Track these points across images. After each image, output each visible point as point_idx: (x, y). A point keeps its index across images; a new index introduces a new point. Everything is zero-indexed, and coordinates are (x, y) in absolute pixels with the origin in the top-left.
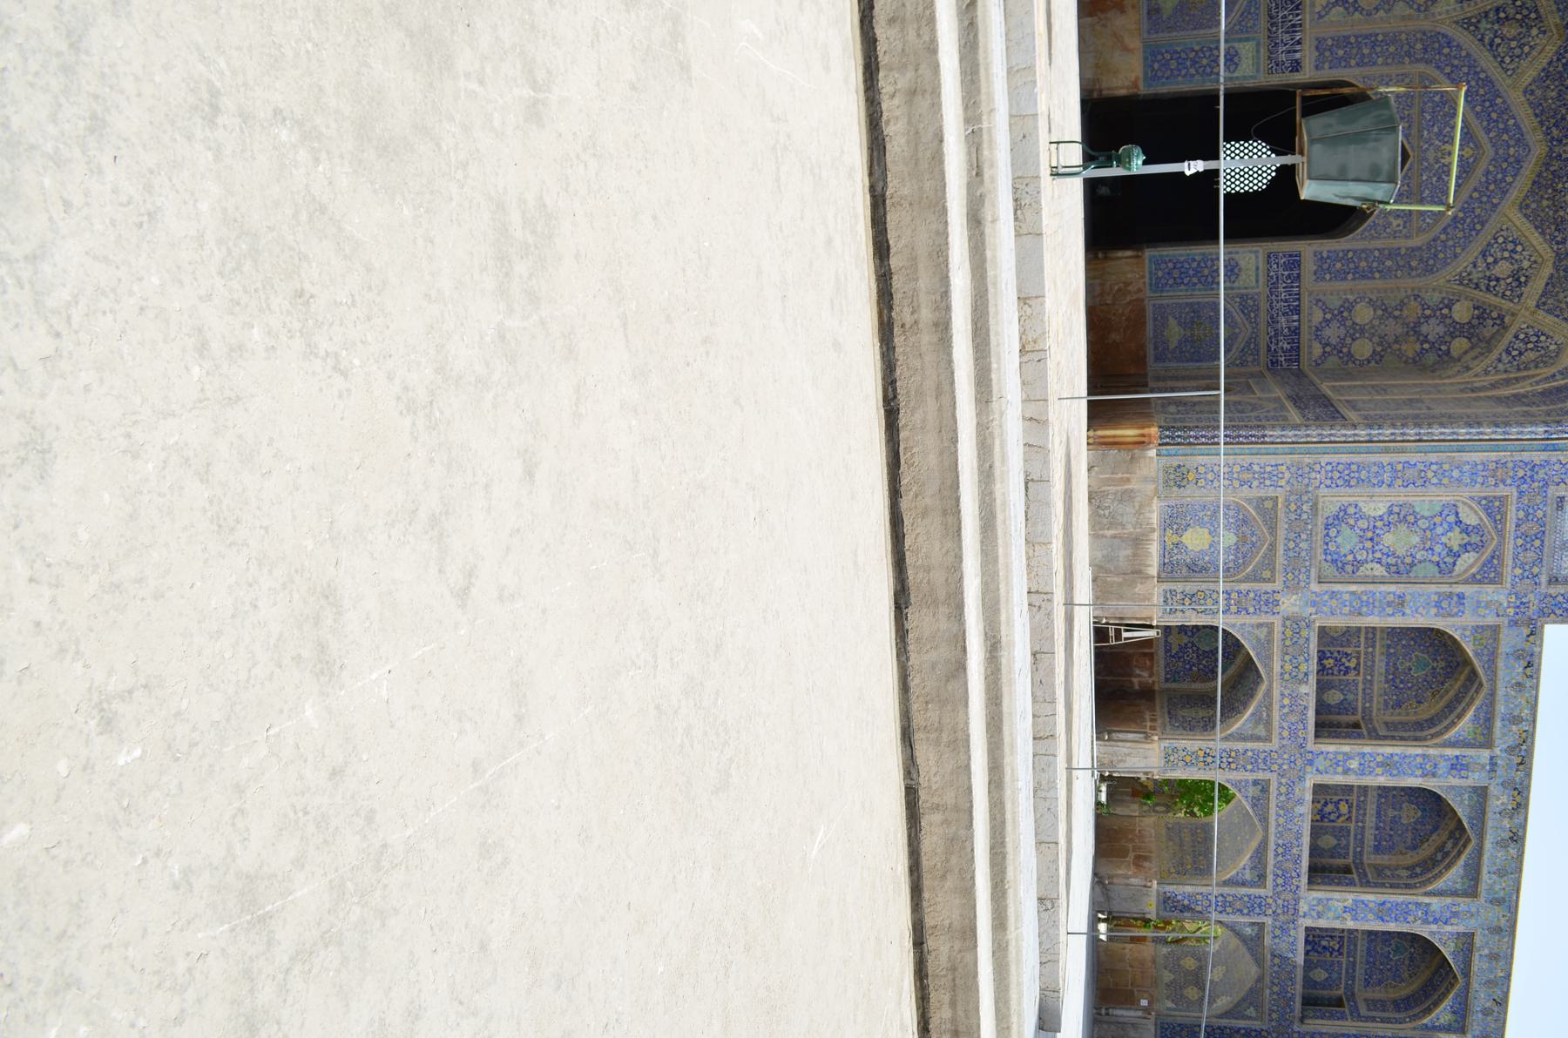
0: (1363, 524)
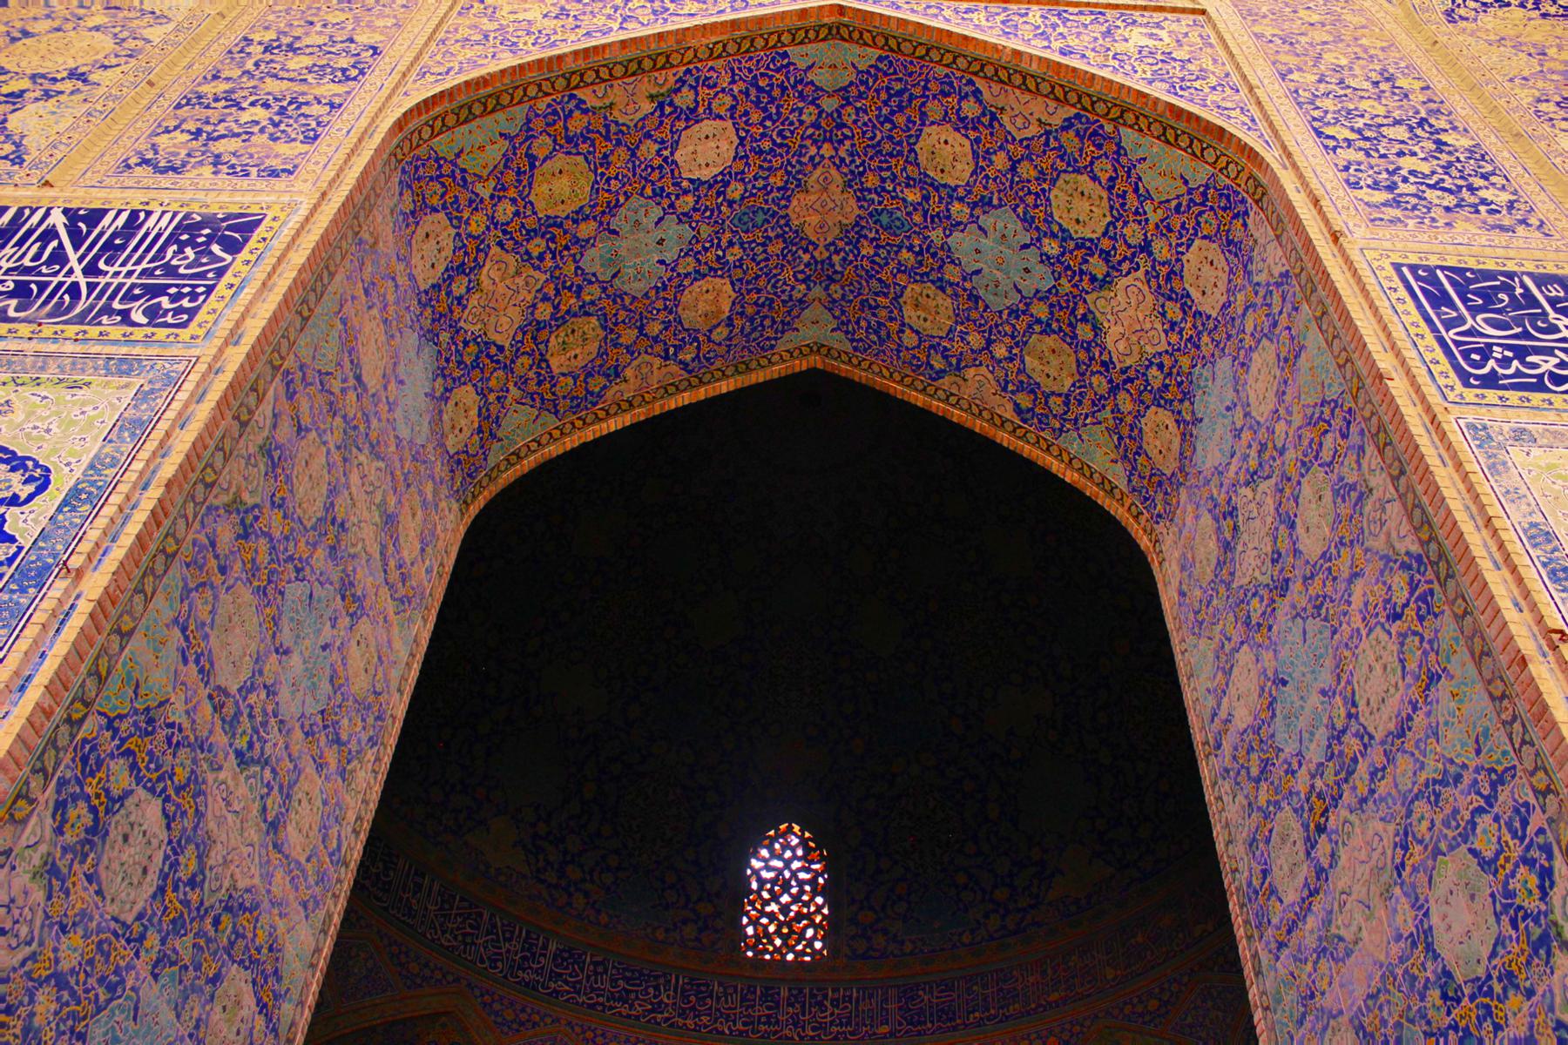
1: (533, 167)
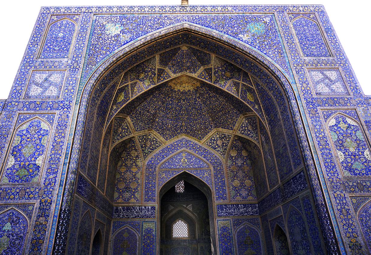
0: (349, 160)
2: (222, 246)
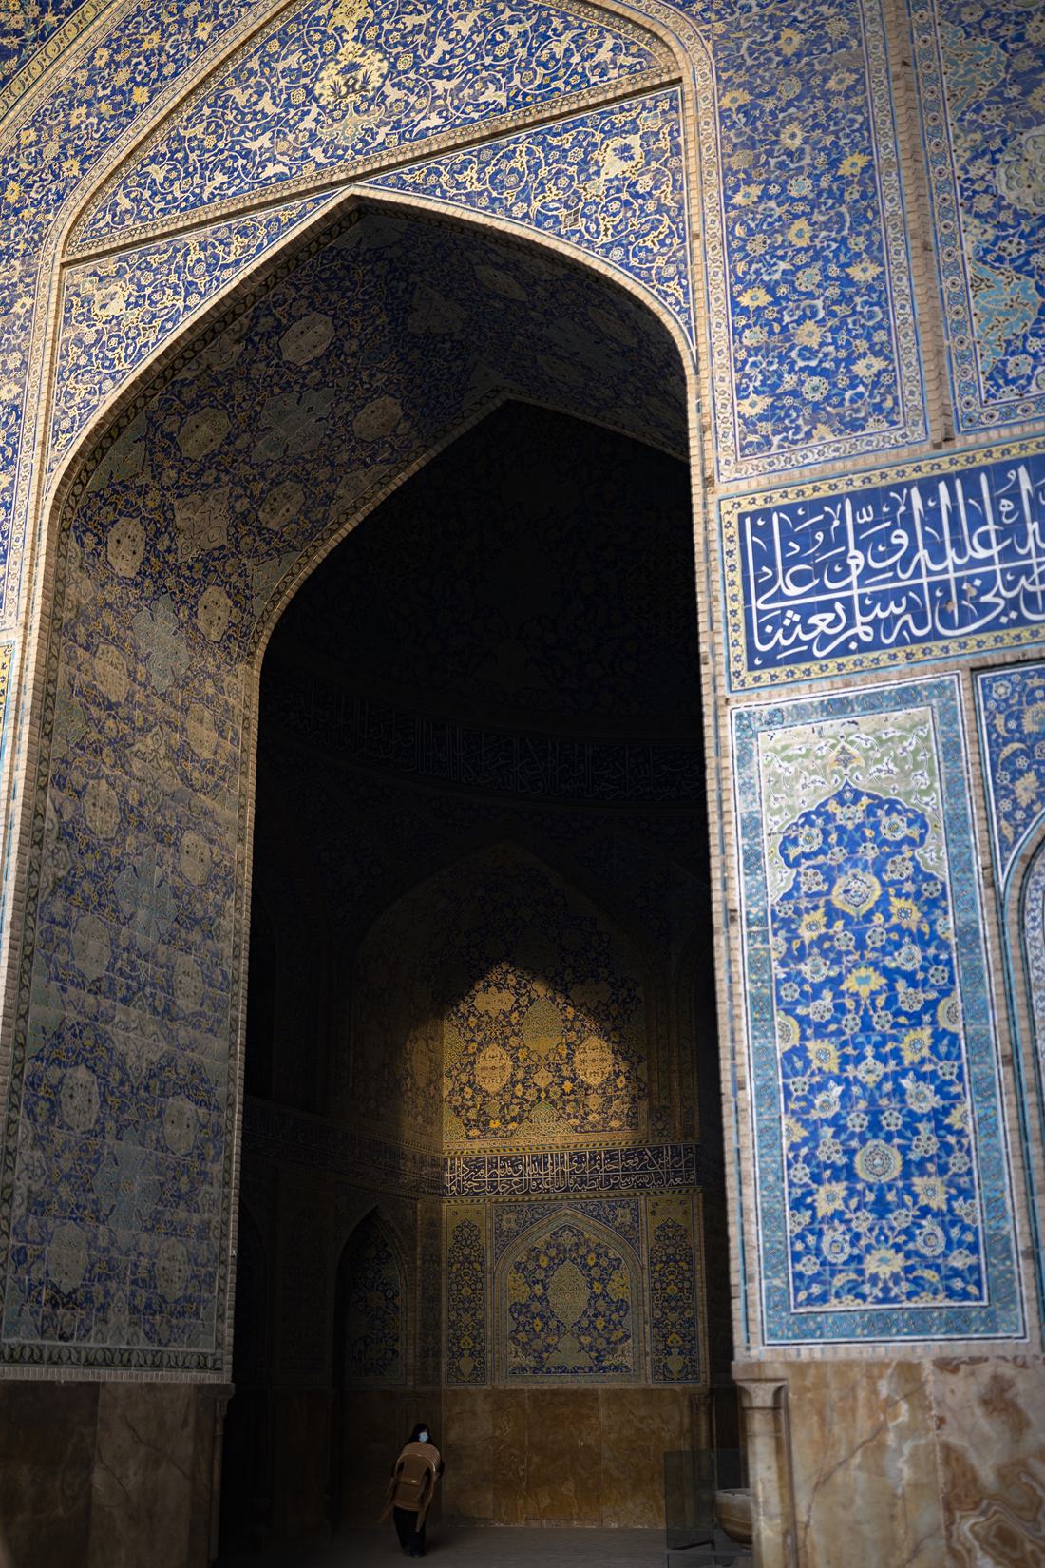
1: (172, 440)
2: (800, 1084)
